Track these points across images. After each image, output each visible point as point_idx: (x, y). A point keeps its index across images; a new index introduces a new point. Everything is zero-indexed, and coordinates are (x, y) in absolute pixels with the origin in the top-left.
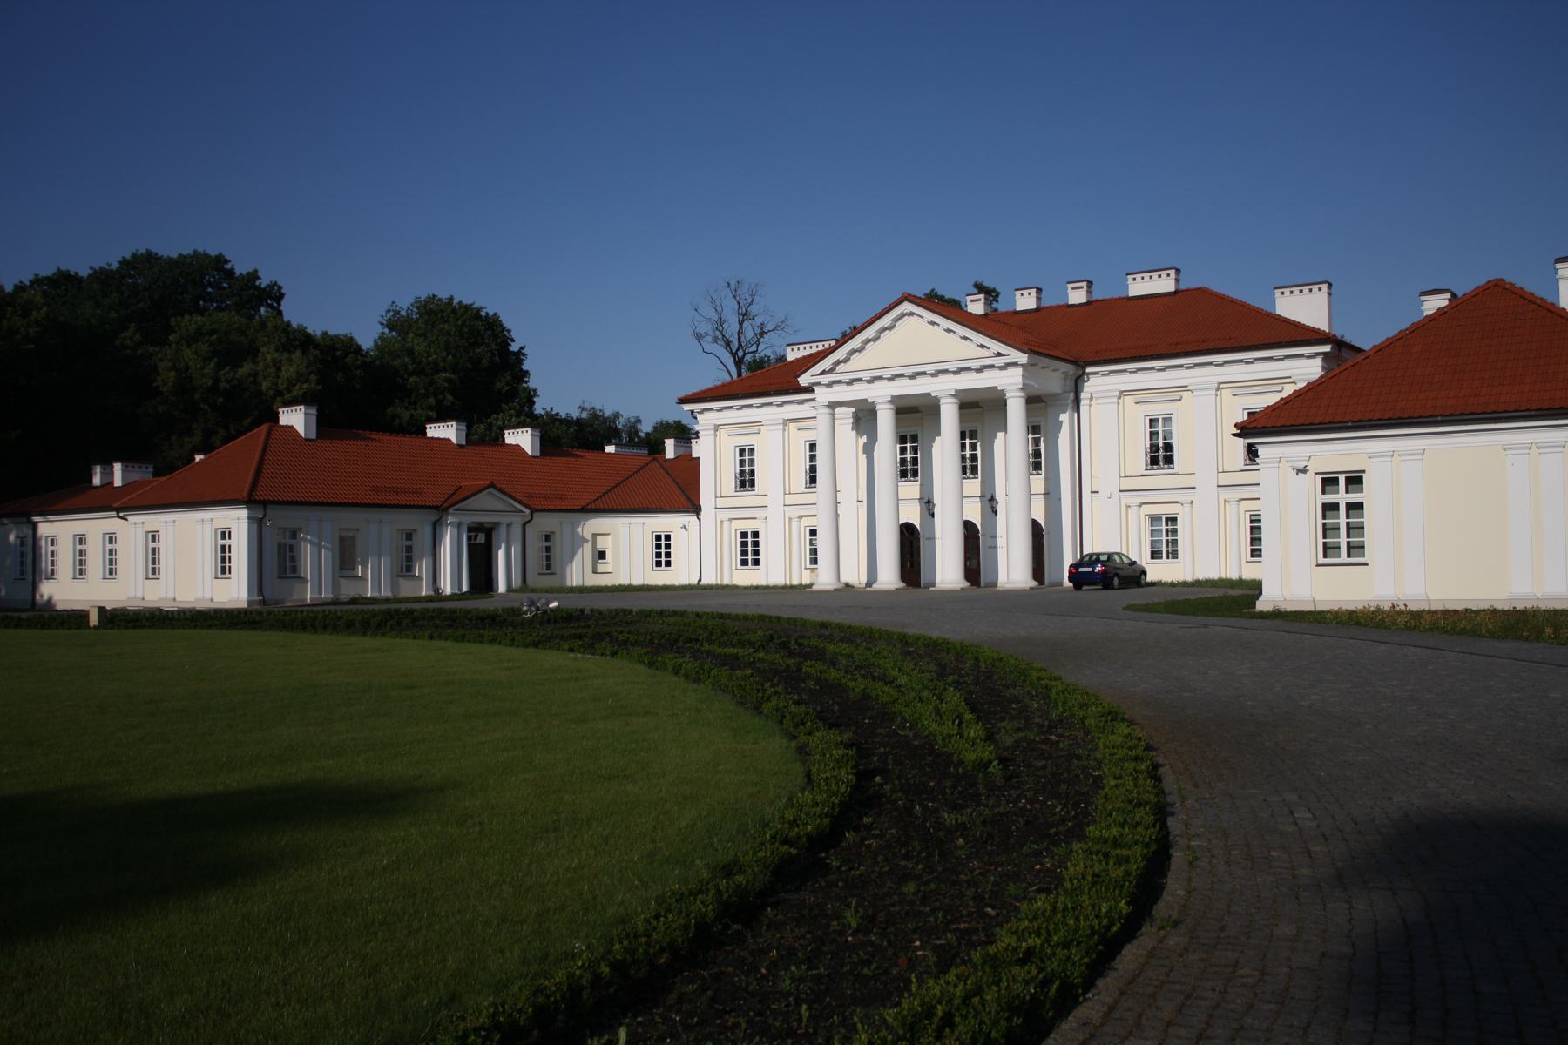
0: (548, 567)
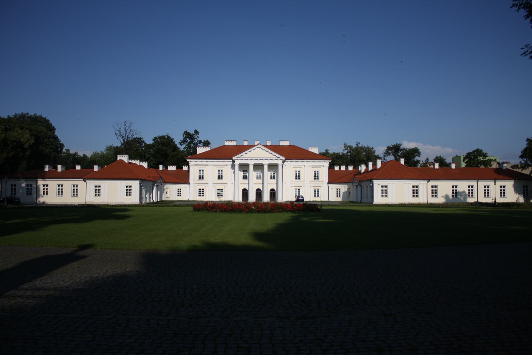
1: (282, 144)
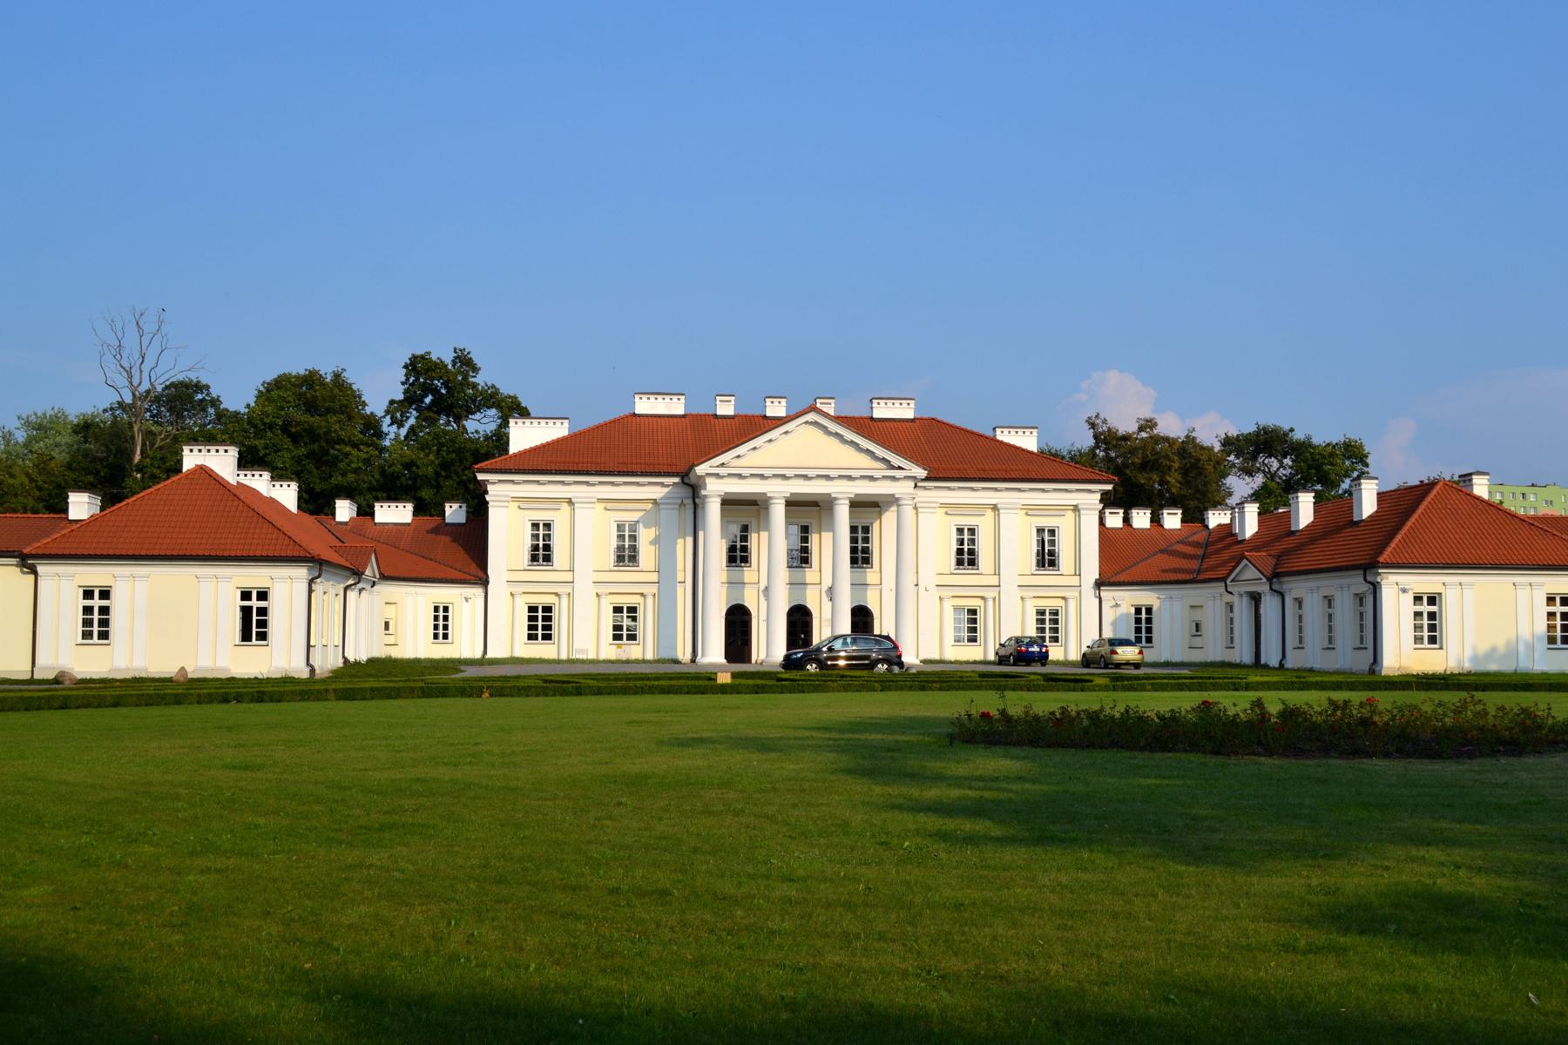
0: (1330, 640)
1: (882, 411)
